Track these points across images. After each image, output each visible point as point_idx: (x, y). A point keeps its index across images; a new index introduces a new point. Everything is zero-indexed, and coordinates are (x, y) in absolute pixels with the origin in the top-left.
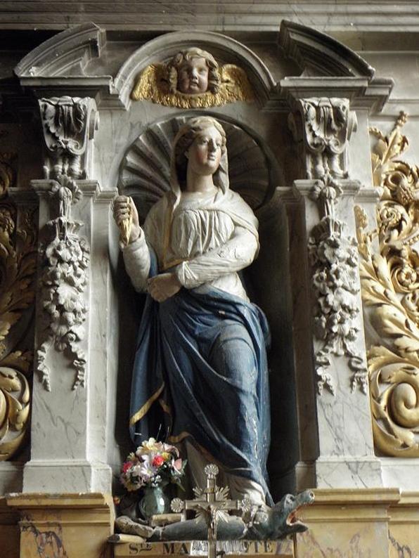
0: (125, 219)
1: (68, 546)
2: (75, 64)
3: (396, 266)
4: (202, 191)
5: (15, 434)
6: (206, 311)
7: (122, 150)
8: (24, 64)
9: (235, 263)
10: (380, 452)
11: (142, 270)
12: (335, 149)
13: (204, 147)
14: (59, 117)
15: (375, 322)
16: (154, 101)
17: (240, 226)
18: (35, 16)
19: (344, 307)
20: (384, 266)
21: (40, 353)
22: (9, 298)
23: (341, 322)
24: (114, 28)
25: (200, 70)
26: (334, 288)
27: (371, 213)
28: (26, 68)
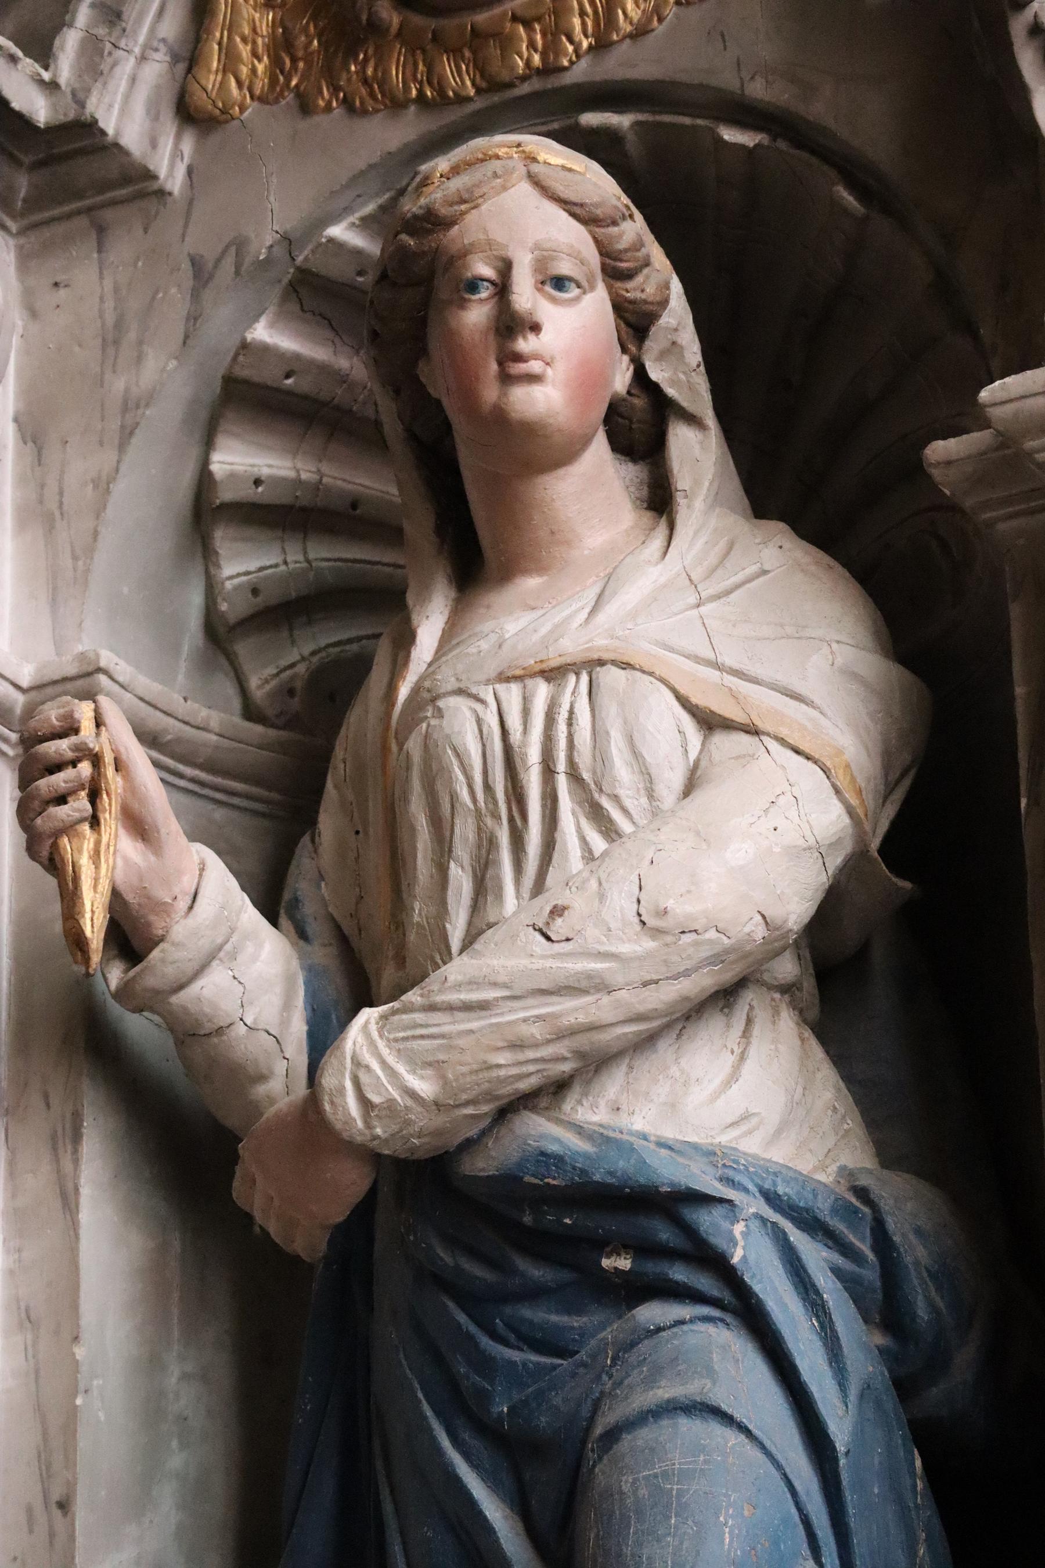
0: (69, 829)
4: (541, 569)
6: (537, 1272)
9: (649, 955)
11: (261, 1090)
13: (476, 315)
16: (305, 107)
17: (728, 725)
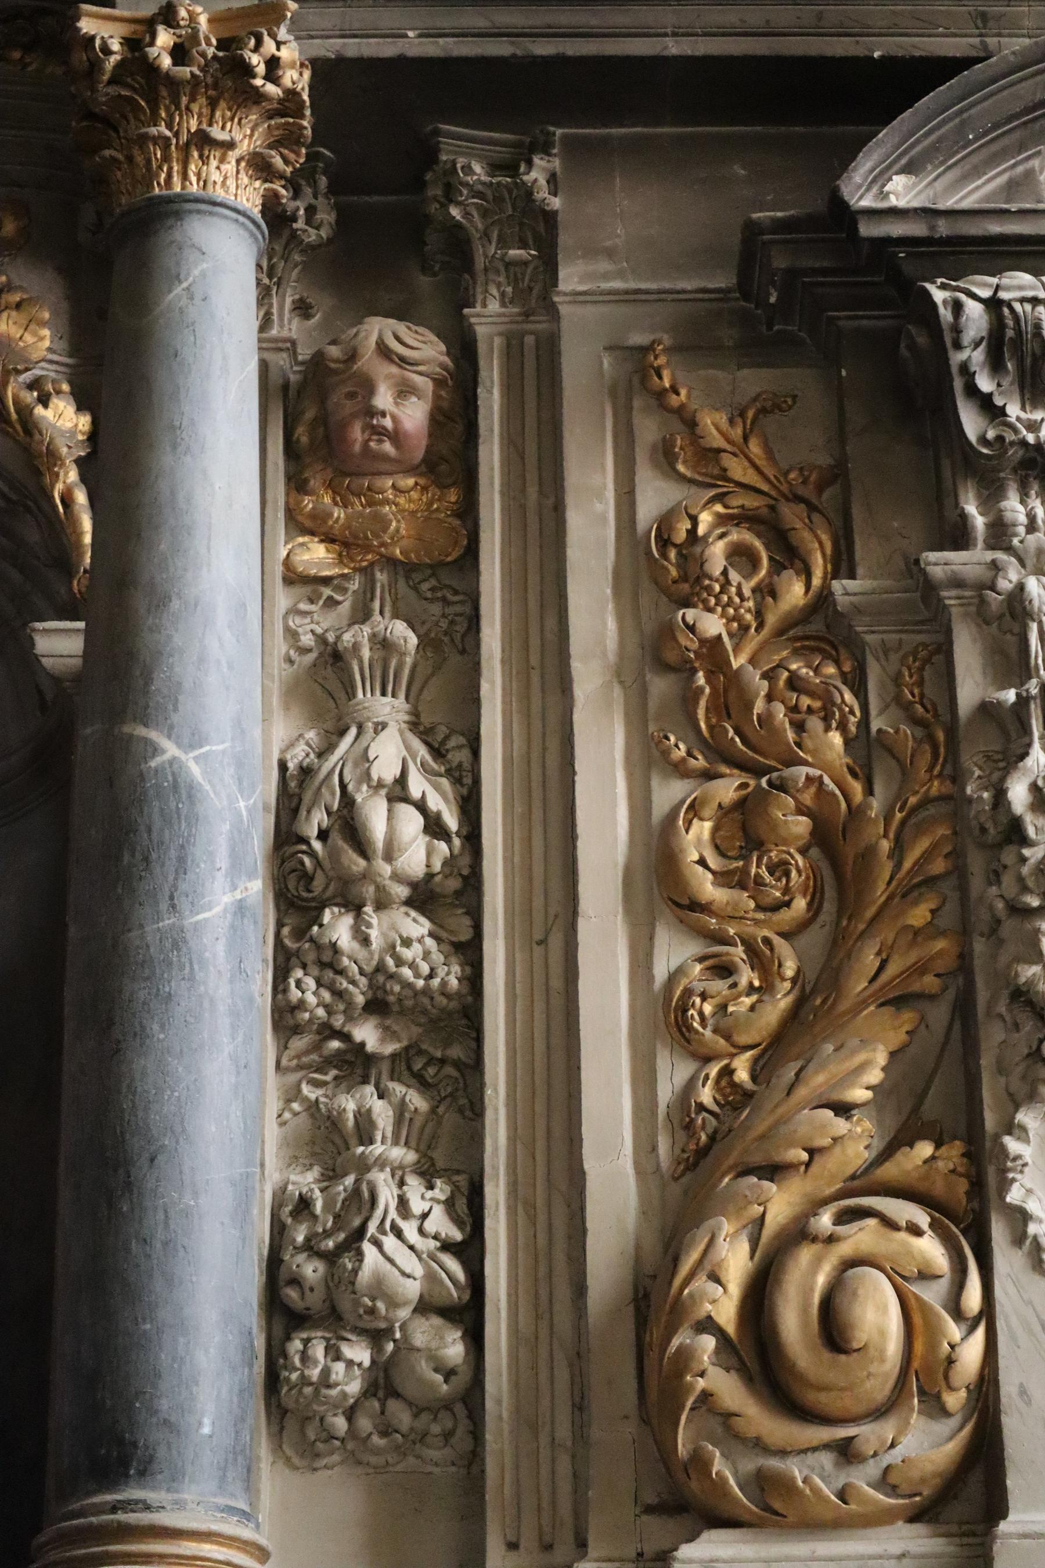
2: (1020, 169)
5: (944, 1427)
8: (869, 165)
21: (1012, 1145)
22: (870, 960)
28: (874, 181)
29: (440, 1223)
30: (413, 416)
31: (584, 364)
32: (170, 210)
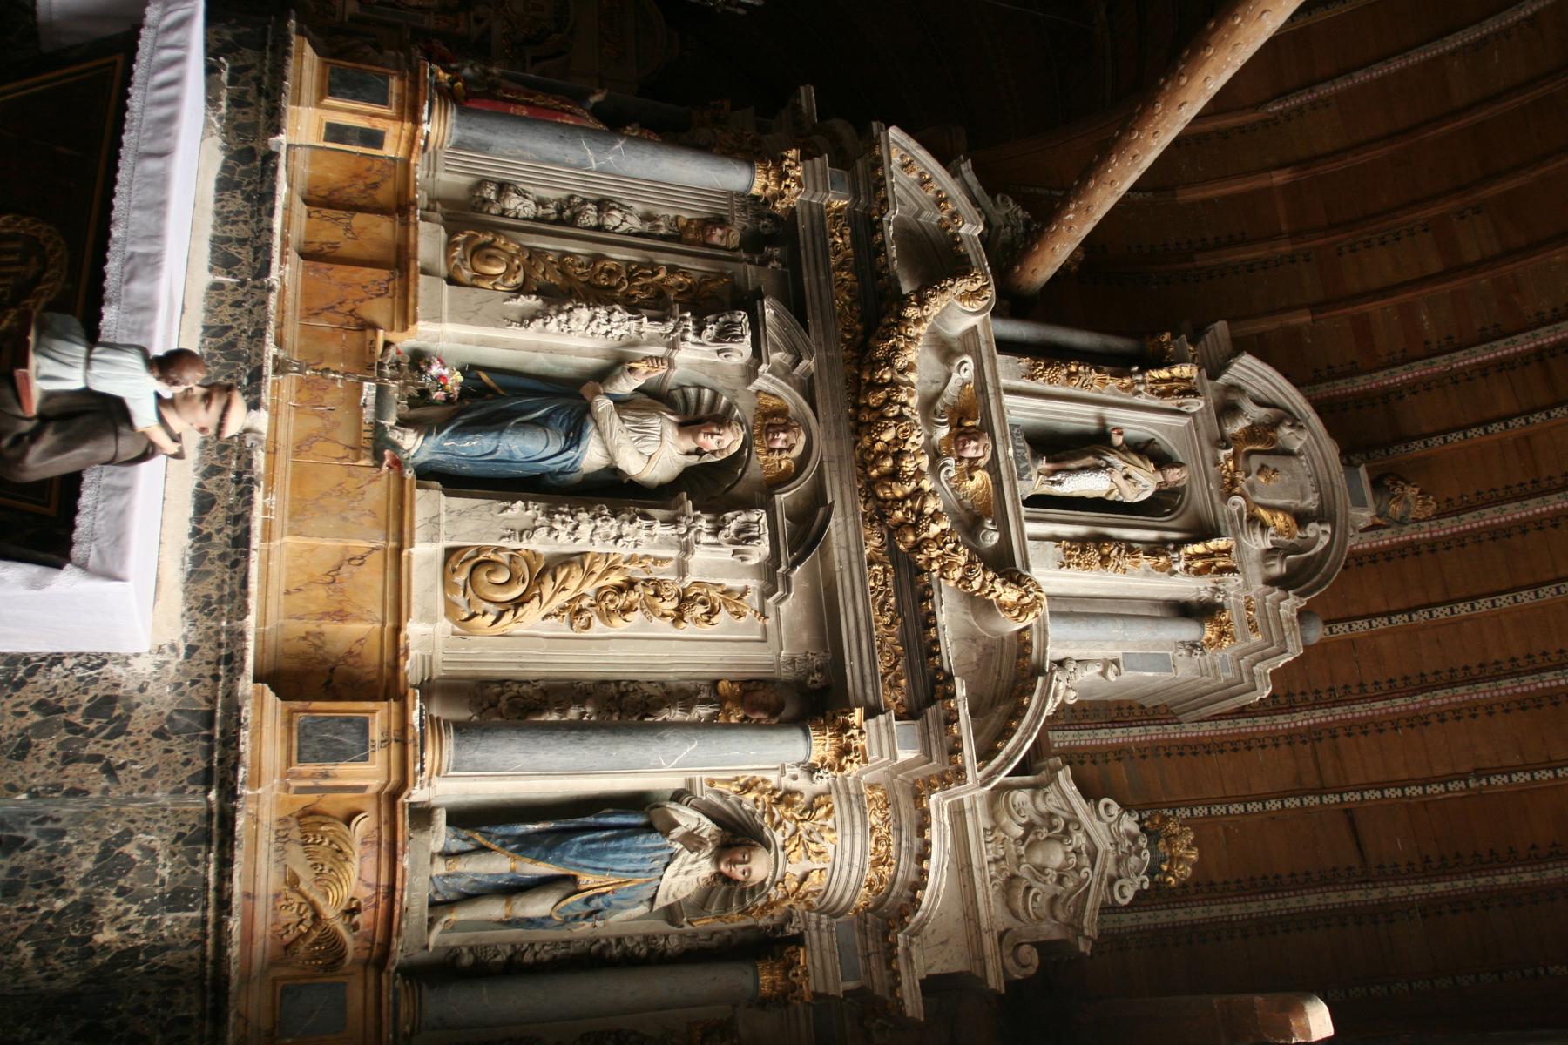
1: (376, 301)
3: (619, 590)
7: (712, 383)
10: (450, 552)
12: (722, 534)
13: (715, 430)
14: (734, 324)
15: (566, 560)
18: (819, 321)
19: (576, 528)
20: (616, 579)
23: (563, 522)
24: (816, 378)
25: (786, 441)
26: (594, 518)
27: (666, 573)
29: (522, 215)
30: (715, 240)
31: (731, 268)
32: (751, 165)
